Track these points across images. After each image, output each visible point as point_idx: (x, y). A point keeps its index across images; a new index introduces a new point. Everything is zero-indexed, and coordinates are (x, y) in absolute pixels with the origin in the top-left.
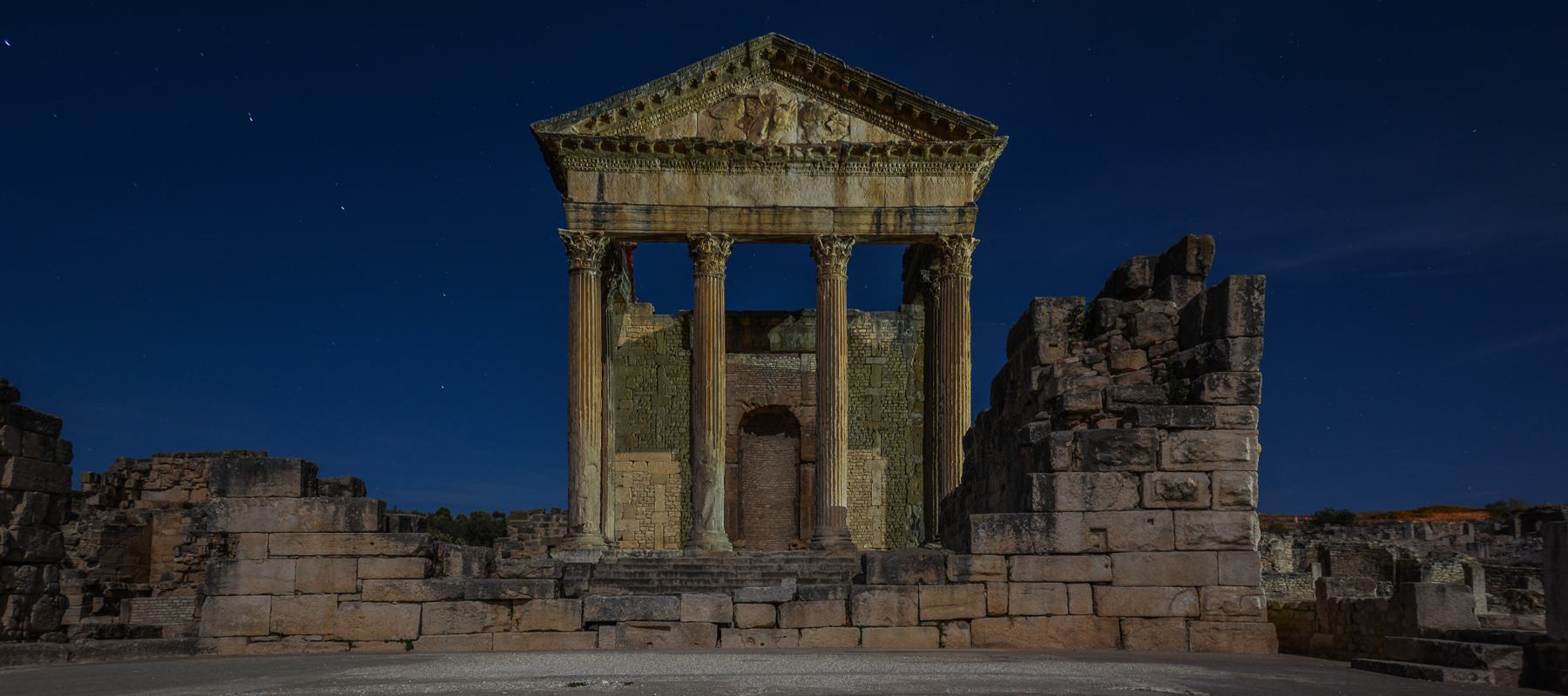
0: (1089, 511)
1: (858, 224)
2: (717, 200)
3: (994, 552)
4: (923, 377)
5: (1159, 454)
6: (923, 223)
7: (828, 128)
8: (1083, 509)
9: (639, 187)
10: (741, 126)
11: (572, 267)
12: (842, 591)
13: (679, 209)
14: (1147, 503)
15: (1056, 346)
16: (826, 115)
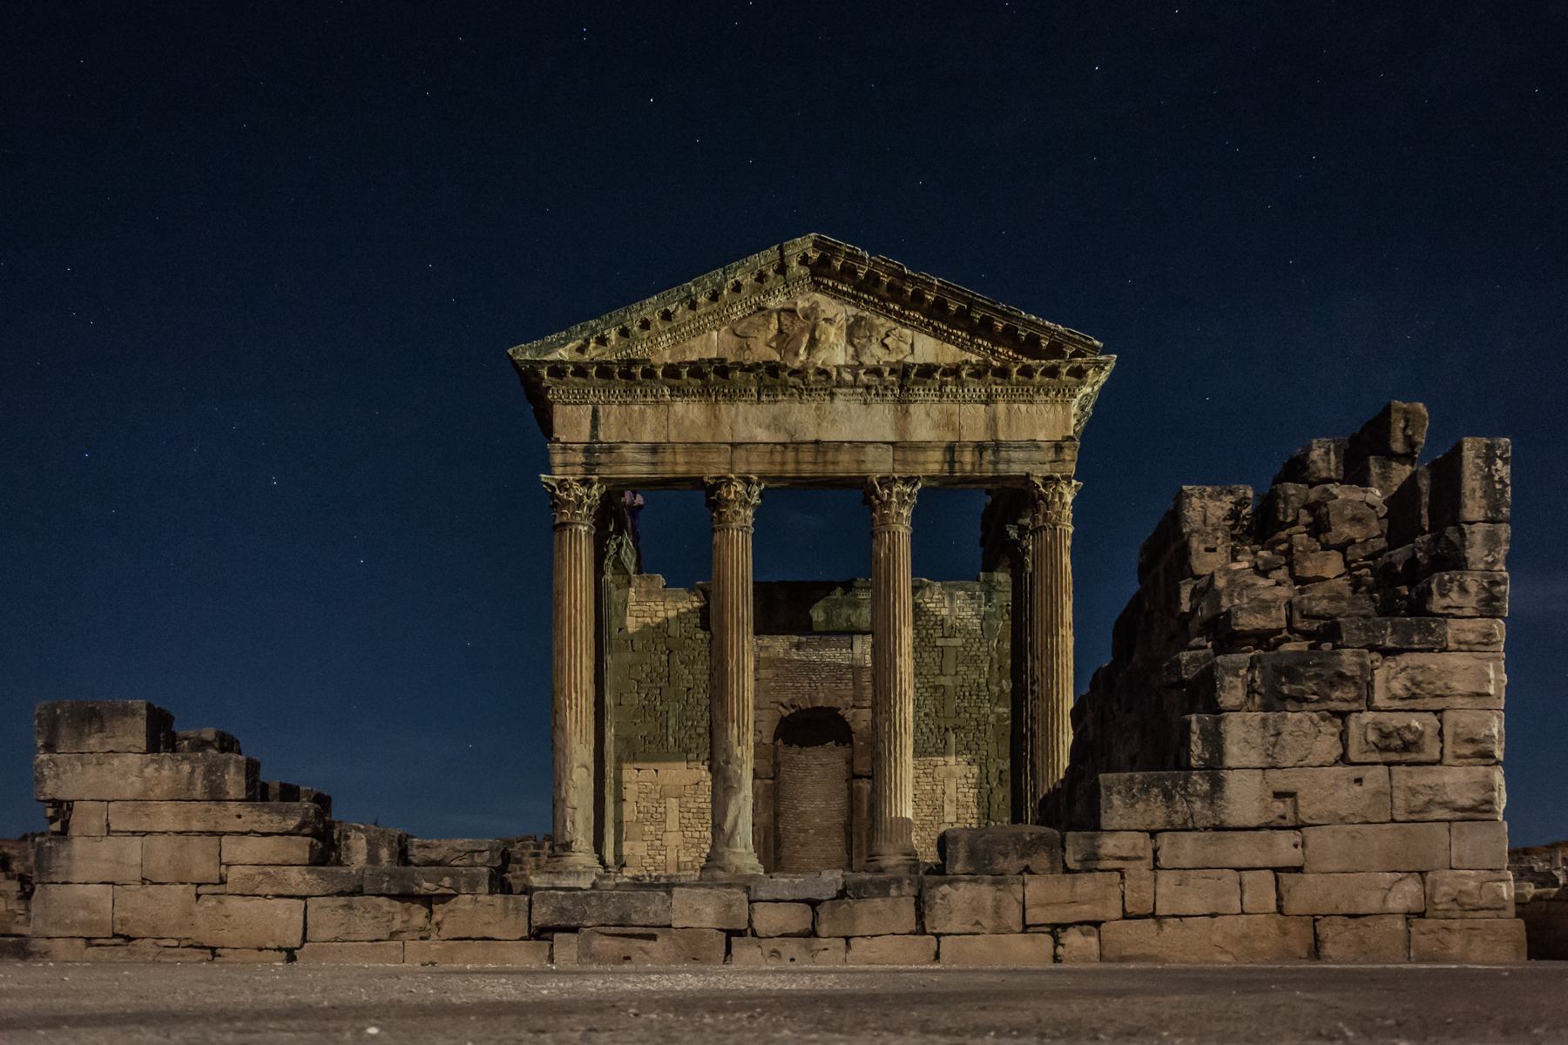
0: (1273, 768)
1: (925, 463)
2: (742, 435)
3: (1135, 828)
4: (1009, 661)
5: (1370, 686)
6: (1009, 461)
7: (885, 346)
8: (1264, 766)
9: (643, 420)
10: (774, 344)
11: (557, 521)
12: (910, 884)
13: (696, 446)
14: (1354, 755)
15: (1214, 550)
16: (883, 331)
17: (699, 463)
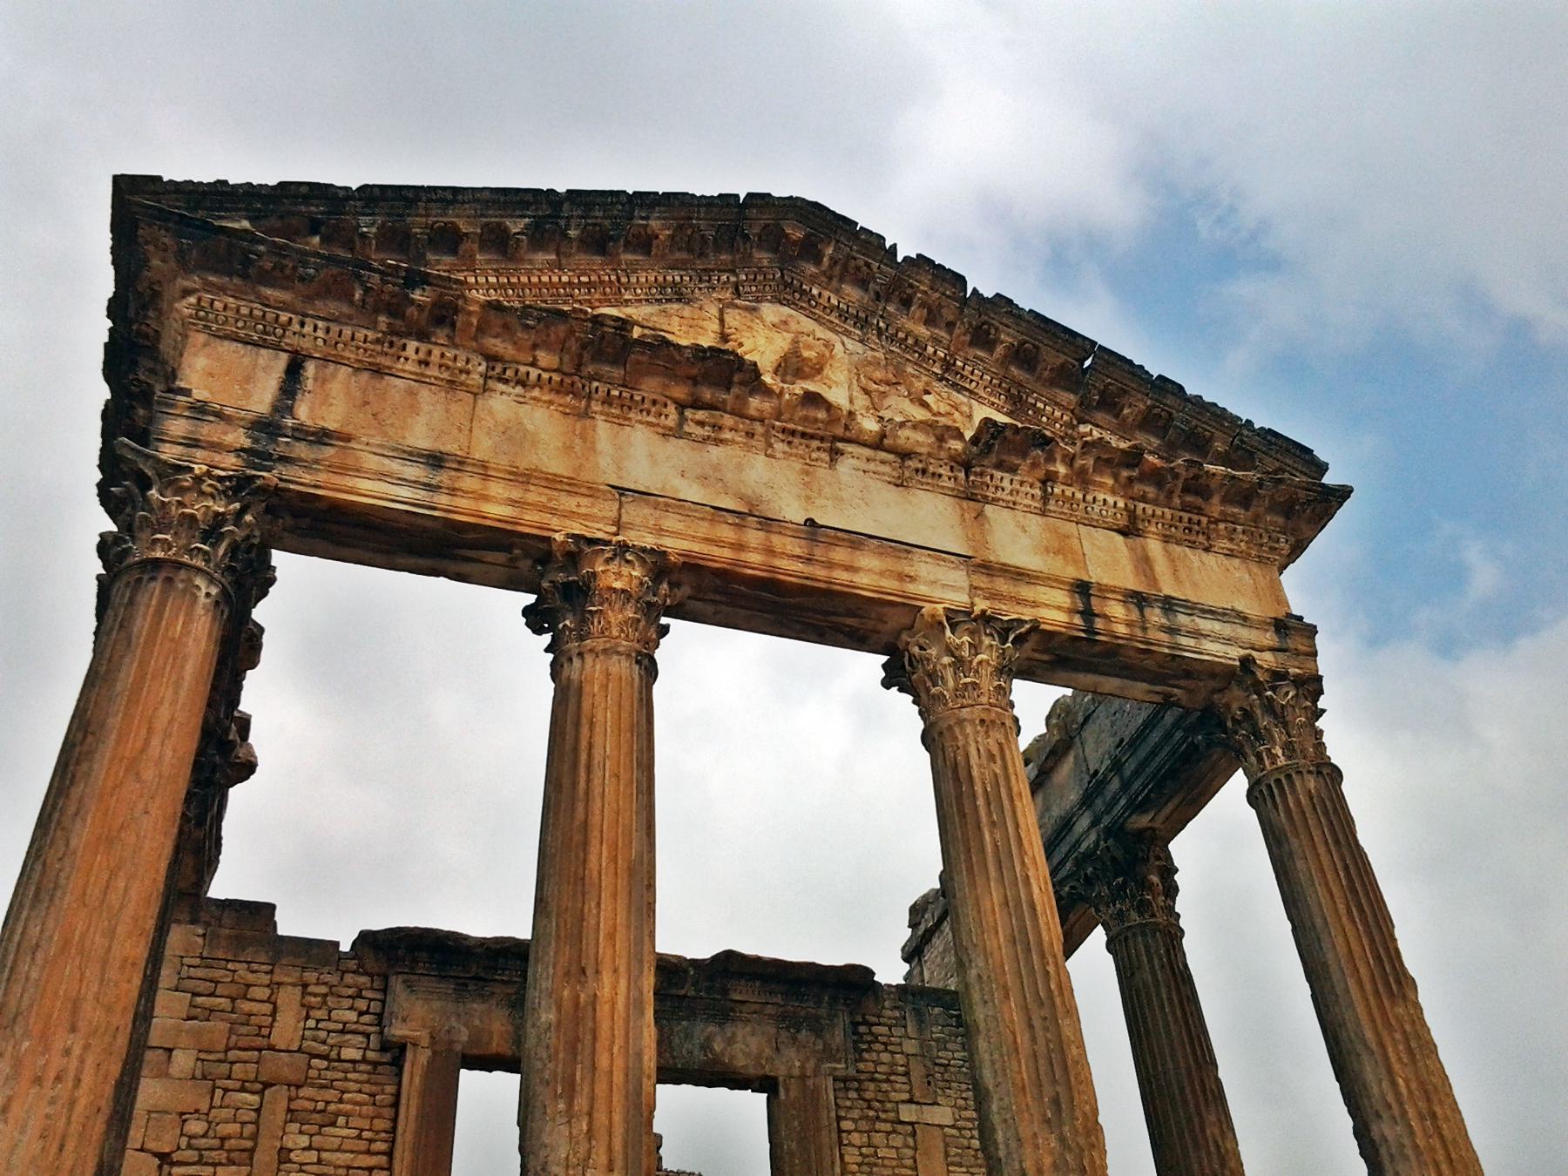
2: (639, 475)
9: (414, 409)
17: (543, 508)
